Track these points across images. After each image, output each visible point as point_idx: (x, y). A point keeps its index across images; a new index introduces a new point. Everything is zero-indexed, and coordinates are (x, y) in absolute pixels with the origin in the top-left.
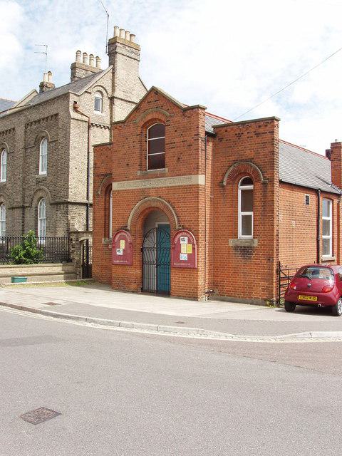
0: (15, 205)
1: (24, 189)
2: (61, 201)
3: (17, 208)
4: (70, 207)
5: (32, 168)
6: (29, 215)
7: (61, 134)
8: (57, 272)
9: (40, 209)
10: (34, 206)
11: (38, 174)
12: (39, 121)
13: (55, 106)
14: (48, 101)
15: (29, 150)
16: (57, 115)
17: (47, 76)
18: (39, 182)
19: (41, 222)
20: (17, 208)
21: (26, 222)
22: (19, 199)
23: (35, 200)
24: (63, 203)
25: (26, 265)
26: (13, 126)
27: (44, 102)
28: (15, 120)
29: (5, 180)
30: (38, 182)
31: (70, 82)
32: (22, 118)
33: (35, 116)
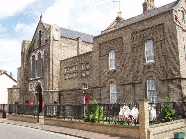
0: (126, 82)
1: (133, 73)
2: (172, 77)
3: (128, 84)
4: (182, 81)
5: (139, 59)
6: (104, 90)
7: (168, 37)
8: (180, 126)
9: (149, 84)
10: (143, 82)
11: (145, 62)
12: (144, 30)
13: (160, 19)
14: (151, 17)
15: (135, 49)
16: (162, 24)
17: (119, 14)
18: (147, 67)
19: (149, 92)
20: (128, 84)
21: (136, 93)
22: (130, 78)
23: (145, 79)
24: (175, 79)
25: (170, 123)
26: (121, 36)
27: (149, 18)
28: (122, 32)
29: (115, 68)
30: (147, 67)
31: (142, 12)
32: (128, 30)
33: (140, 27)
